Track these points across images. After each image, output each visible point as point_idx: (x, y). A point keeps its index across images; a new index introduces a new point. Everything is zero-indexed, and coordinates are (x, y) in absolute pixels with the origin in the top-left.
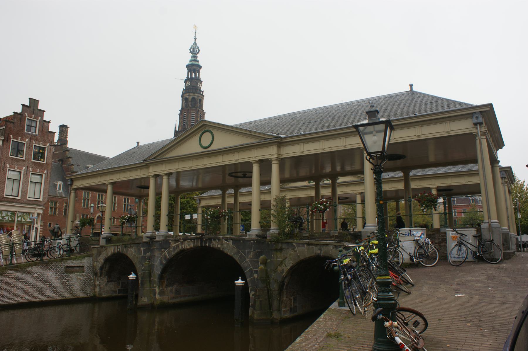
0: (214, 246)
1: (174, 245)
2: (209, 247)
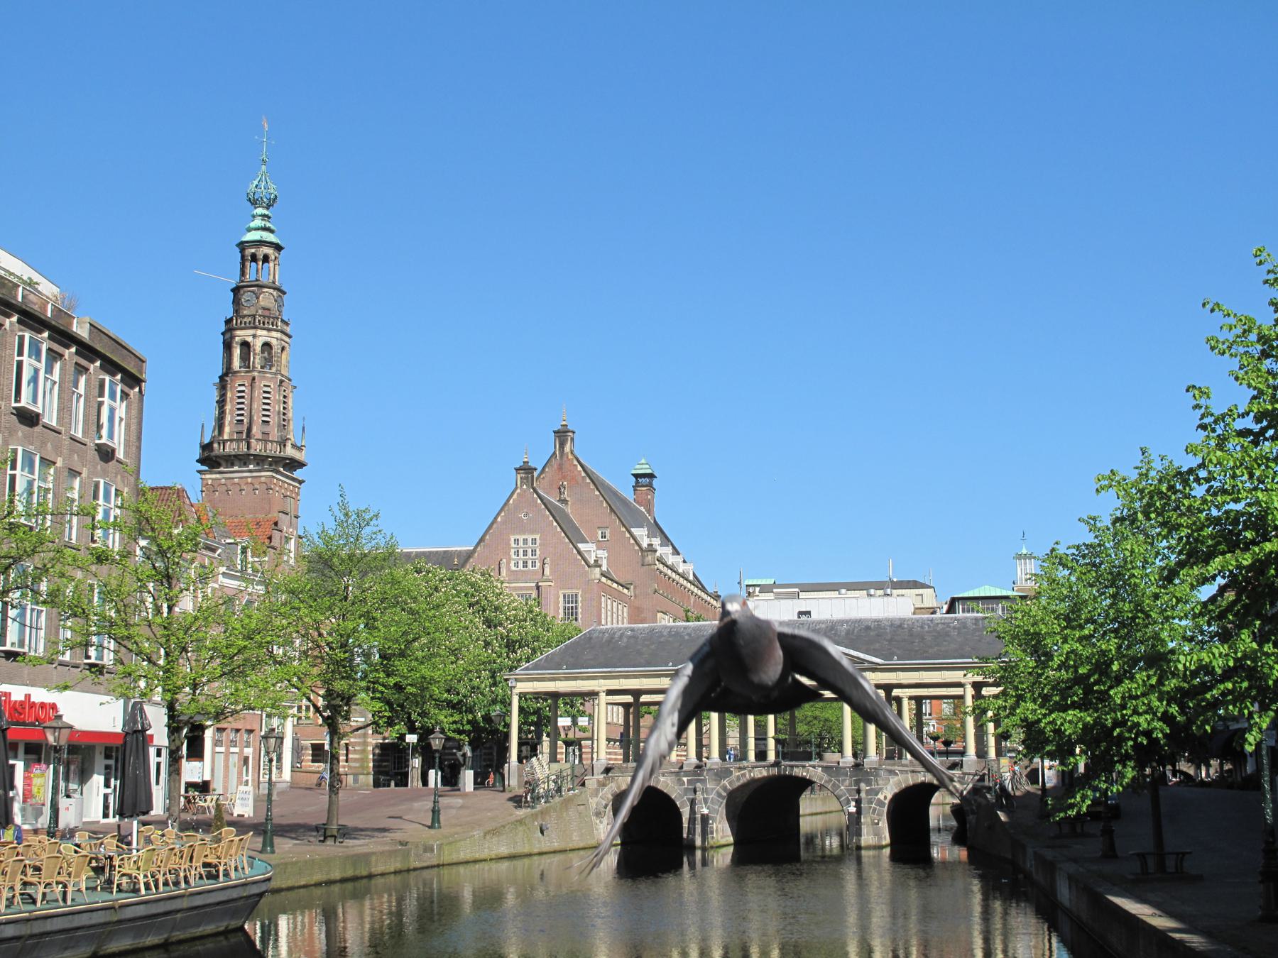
0: (797, 774)
1: (738, 774)
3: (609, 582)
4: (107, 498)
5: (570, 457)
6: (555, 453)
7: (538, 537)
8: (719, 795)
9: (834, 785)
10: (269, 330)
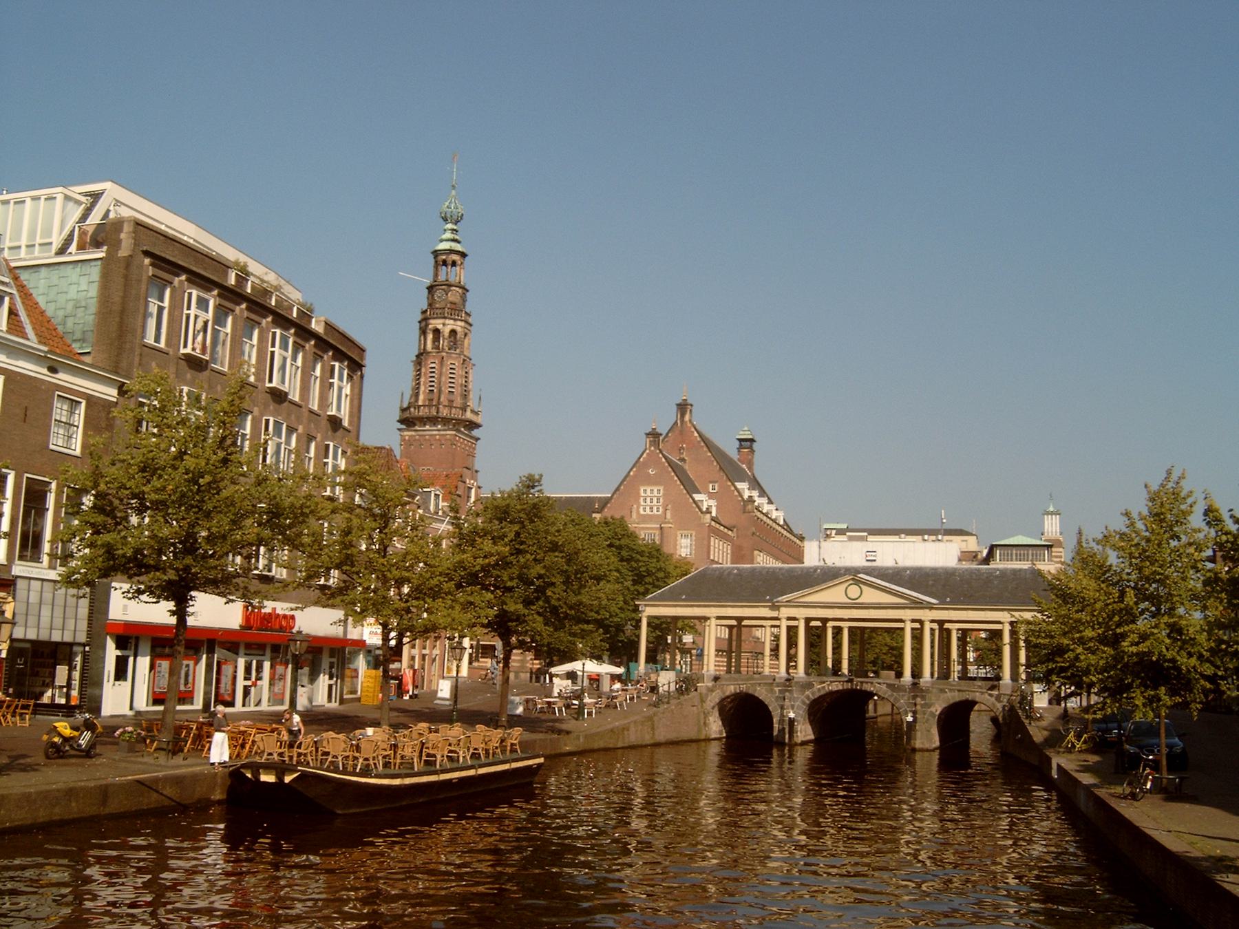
2: (861, 691)
3: (717, 526)
4: (335, 458)
5: (689, 425)
6: (676, 422)
7: (661, 488)
8: (804, 703)
9: (896, 699)
10: (455, 320)
